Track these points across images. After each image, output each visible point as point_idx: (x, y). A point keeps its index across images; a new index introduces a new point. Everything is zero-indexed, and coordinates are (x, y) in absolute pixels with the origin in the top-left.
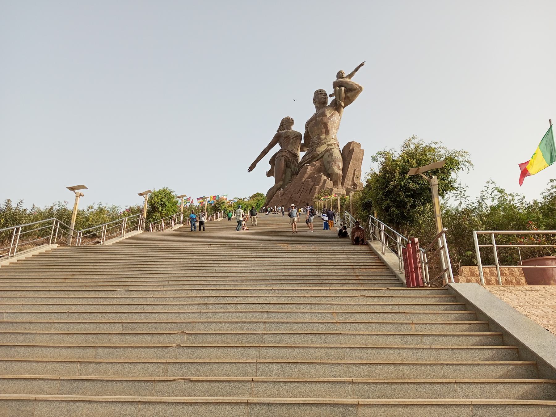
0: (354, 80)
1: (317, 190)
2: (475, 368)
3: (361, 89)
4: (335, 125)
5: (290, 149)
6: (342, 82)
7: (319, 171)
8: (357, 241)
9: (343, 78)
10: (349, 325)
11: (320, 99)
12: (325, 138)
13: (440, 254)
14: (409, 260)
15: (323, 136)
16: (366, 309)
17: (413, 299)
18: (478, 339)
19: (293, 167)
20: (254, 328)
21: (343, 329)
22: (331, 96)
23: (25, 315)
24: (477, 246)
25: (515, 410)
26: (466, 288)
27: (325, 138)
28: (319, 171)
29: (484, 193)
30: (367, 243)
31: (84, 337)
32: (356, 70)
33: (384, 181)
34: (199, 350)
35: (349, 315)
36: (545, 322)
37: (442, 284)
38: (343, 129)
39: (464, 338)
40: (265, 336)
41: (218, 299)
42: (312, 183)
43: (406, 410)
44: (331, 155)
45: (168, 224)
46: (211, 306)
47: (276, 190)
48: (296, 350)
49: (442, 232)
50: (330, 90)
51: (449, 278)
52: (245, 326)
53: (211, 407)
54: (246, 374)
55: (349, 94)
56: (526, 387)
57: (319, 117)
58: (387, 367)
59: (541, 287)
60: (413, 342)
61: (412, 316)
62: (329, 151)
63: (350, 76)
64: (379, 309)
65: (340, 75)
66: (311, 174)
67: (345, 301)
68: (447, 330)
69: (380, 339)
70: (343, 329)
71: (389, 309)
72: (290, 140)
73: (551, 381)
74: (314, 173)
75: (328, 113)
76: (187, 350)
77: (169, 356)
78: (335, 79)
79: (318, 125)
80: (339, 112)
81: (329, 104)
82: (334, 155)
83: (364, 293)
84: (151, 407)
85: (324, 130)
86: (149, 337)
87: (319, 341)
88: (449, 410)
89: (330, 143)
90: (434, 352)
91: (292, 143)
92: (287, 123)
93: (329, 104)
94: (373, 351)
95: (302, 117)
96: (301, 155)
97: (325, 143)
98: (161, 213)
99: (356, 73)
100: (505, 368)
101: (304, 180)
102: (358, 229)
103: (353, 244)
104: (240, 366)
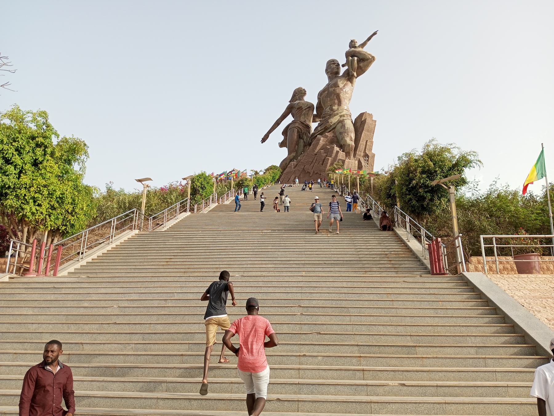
0: (367, 50)
1: (330, 161)
2: (478, 328)
4: (347, 95)
5: (302, 120)
6: (355, 51)
7: (332, 142)
8: (384, 228)
9: (356, 47)
10: (400, 302)
11: (332, 69)
12: (338, 109)
13: (456, 251)
14: (433, 252)
15: (335, 107)
16: (408, 291)
17: (439, 284)
18: (481, 311)
19: (305, 137)
20: (344, 304)
21: (396, 305)
22: (343, 66)
23: (189, 294)
24: (483, 246)
25: (498, 349)
26: (474, 277)
27: (338, 109)
28: (332, 142)
29: (492, 186)
30: (393, 230)
31: (239, 308)
32: (369, 39)
33: (408, 178)
34: (314, 317)
35: (398, 295)
36: (523, 300)
37: (457, 272)
38: (356, 99)
39: (472, 311)
40: (350, 309)
41: (307, 283)
42: (325, 155)
43: (441, 349)
44: (343, 126)
45: (207, 203)
46: (305, 288)
47: (289, 160)
48: (372, 317)
49: (459, 236)
50: (342, 60)
51: (463, 268)
52: (334, 302)
53: (338, 347)
54: (347, 331)
55: (361, 64)
56: (506, 338)
57: (331, 87)
58: (428, 327)
59: (525, 275)
60: (441, 313)
61: (439, 296)
62: (341, 122)
63: (363, 45)
64: (416, 291)
65: (352, 44)
66: (324, 145)
67: (392, 285)
68: (461, 305)
69: (421, 311)
70: (396, 305)
71: (423, 291)
72: (303, 111)
73: (520, 335)
74: (327, 145)
75: (341, 84)
76: (307, 317)
77: (296, 320)
78: (347, 48)
79: (330, 96)
80: (352, 82)
81: (341, 74)
82: (346, 126)
83: (405, 279)
84: (306, 347)
85: (336, 101)
86: (279, 309)
87: (383, 312)
88: (464, 349)
89: (342, 114)
90: (454, 319)
91: (304, 114)
92: (299, 94)
93: (341, 74)
94: (418, 318)
95: (314, 86)
96: (314, 126)
97: (337, 114)
98: (201, 195)
99: (369, 43)
100: (496, 328)
102: (384, 217)
103: (380, 230)
104: (343, 326)
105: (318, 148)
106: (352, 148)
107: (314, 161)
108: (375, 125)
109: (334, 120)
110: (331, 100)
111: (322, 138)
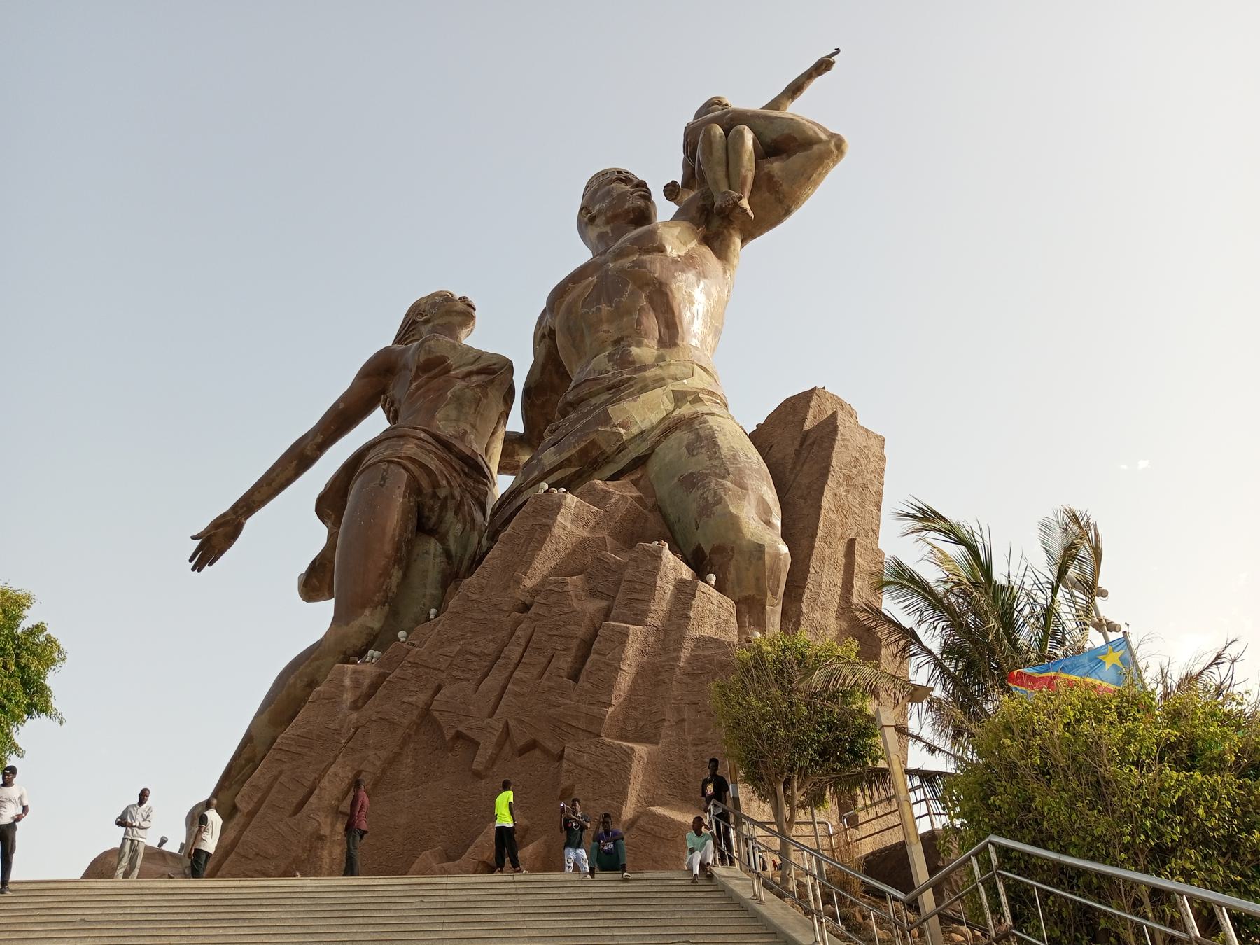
3: (839, 144)
5: (445, 429)
7: (632, 533)
11: (614, 207)
15: (646, 351)
19: (454, 527)
27: (661, 358)
32: (795, 89)
44: (705, 442)
50: (661, 166)
62: (689, 430)
66: (580, 546)
72: (449, 383)
80: (722, 254)
82: (720, 439)
85: (651, 323)
89: (687, 384)
91: (459, 400)
97: (660, 382)
101: (529, 583)
105: (544, 562)
106: (775, 570)
107: (514, 651)
108: (883, 459)
109: (642, 413)
110: (620, 313)
111: (571, 500)
